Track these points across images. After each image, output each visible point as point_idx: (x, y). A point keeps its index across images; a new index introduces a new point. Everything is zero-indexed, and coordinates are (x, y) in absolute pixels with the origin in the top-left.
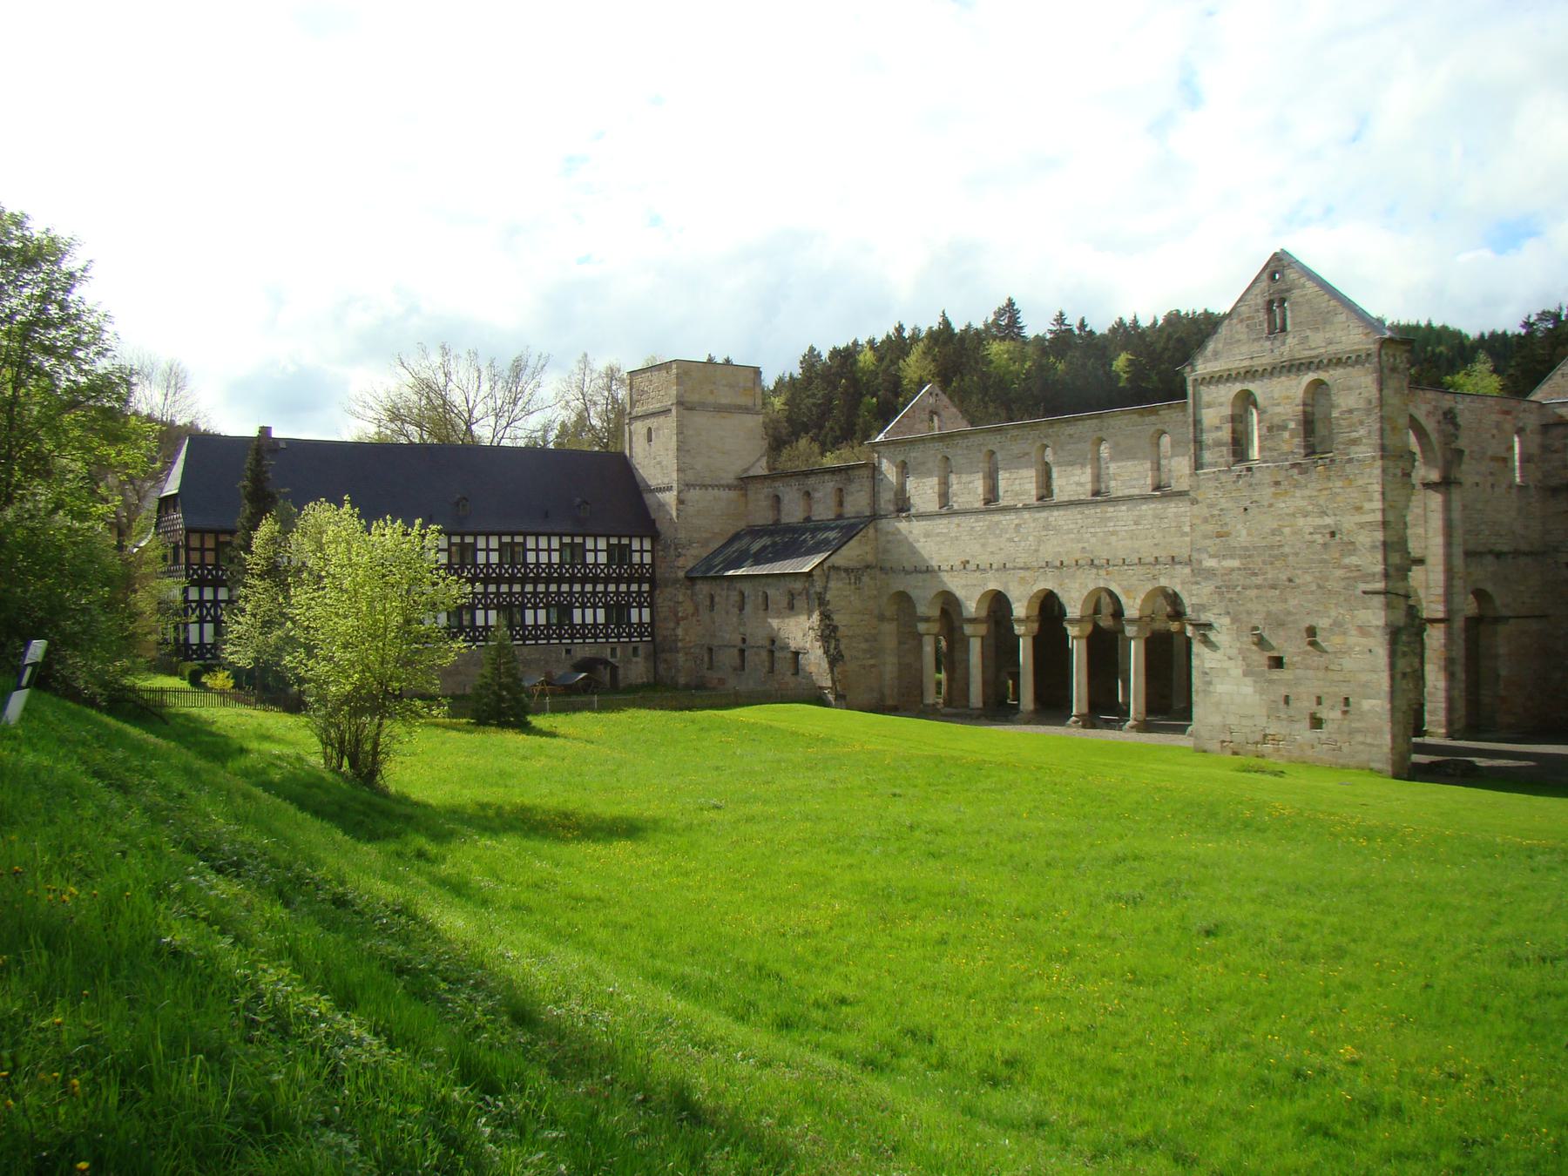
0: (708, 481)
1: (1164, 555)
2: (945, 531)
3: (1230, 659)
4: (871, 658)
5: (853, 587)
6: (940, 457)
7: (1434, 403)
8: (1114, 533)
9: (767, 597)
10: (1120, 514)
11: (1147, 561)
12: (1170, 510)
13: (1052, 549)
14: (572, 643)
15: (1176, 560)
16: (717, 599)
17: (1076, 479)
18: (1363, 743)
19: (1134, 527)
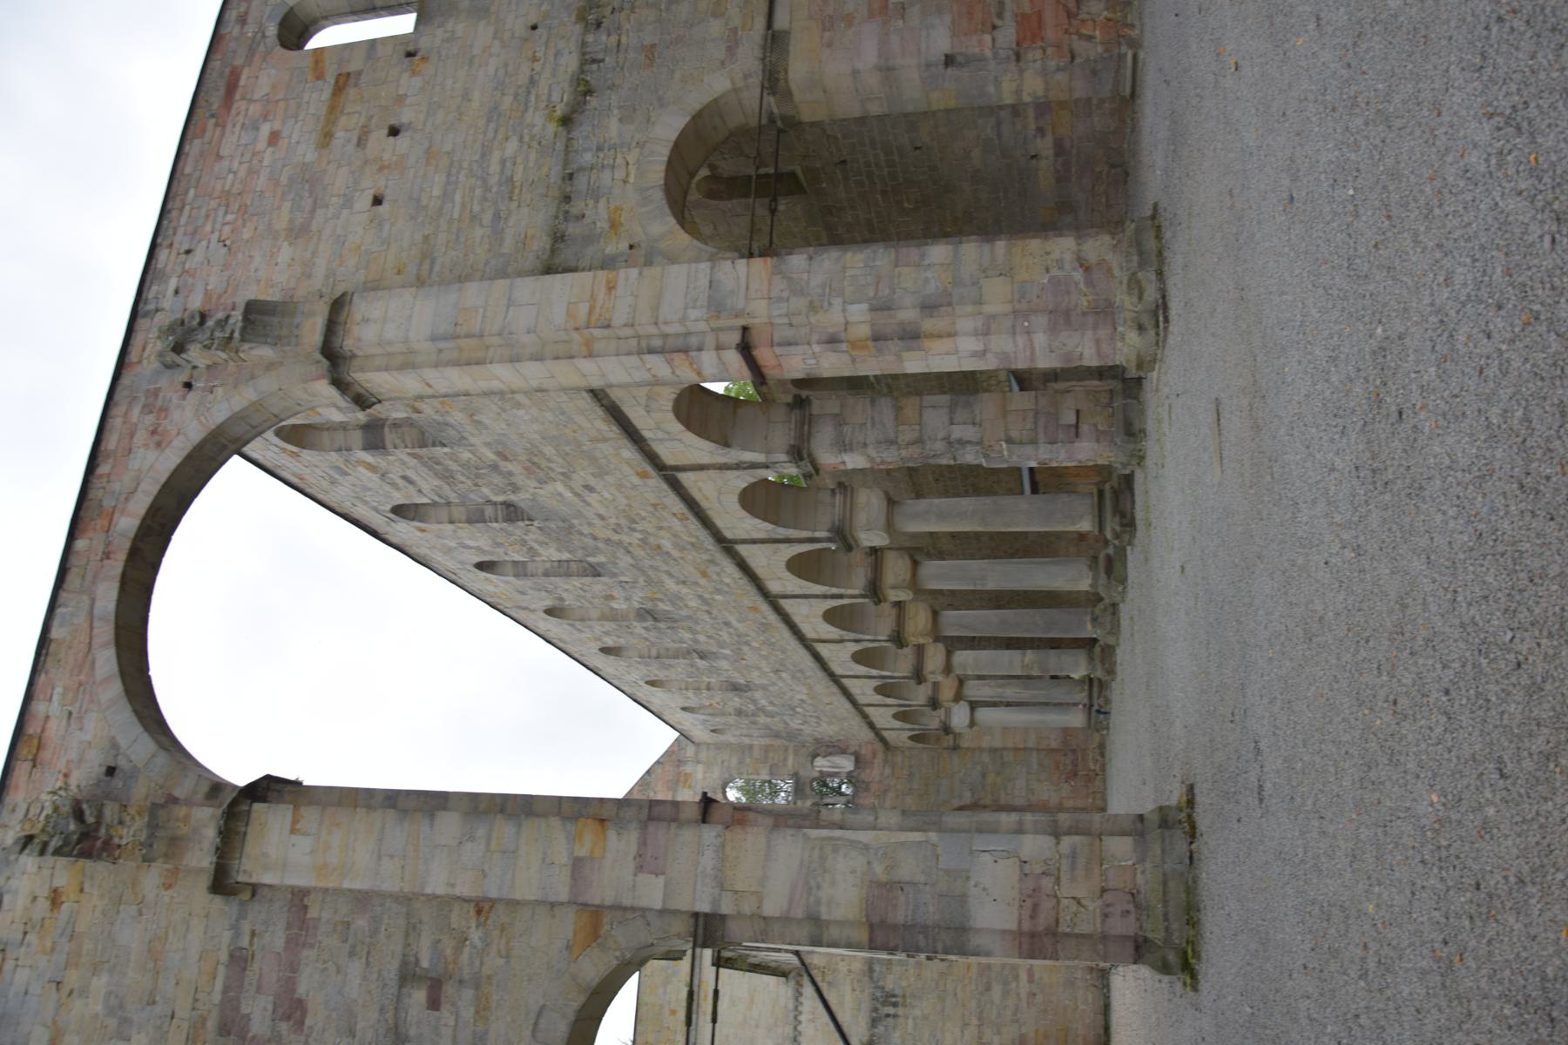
0: (789, 1030)
4: (1017, 978)
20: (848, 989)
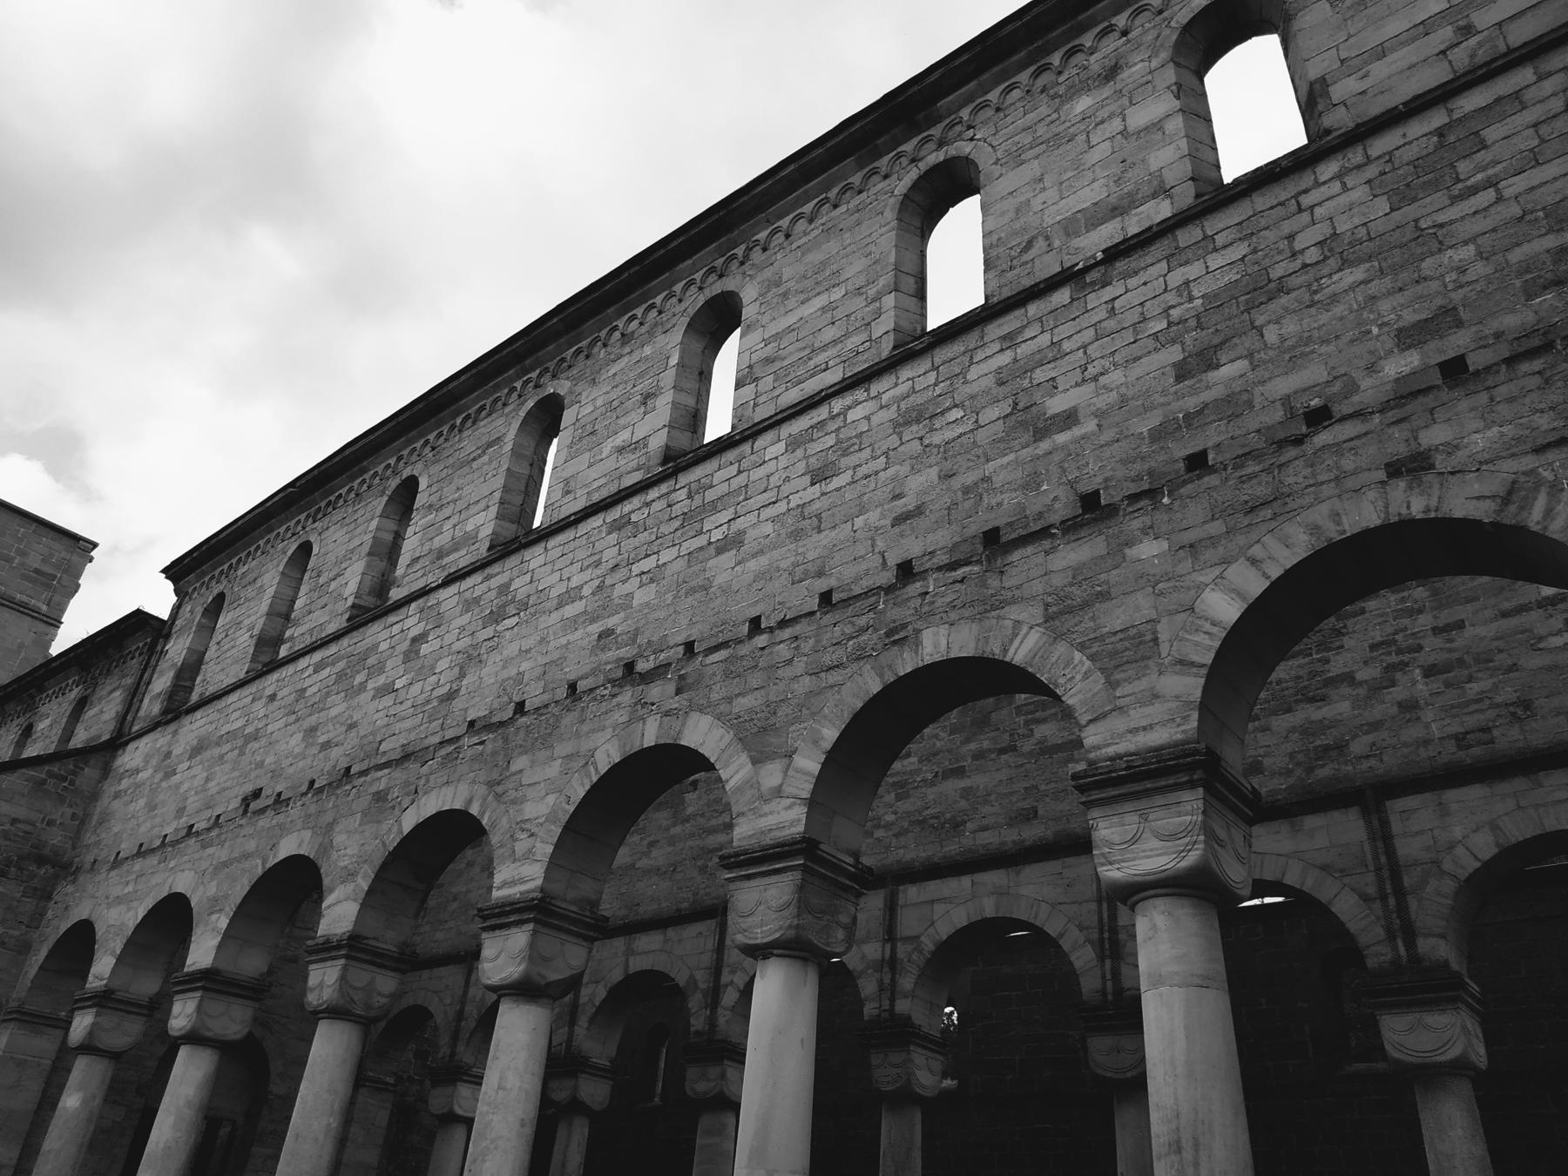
10: (757, 474)
12: (973, 374)
17: (623, 437)
20: (21, 812)
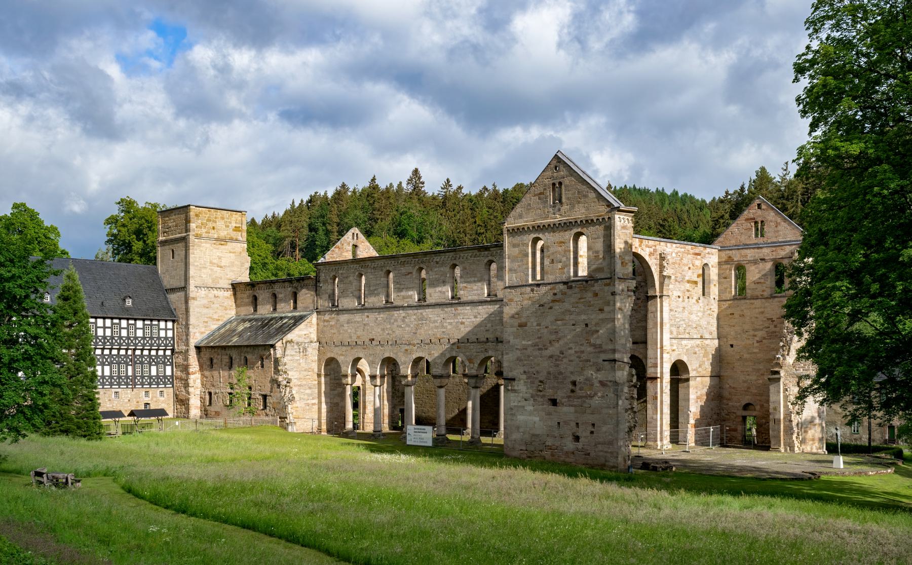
1: (491, 336)
2: (360, 320)
3: (526, 400)
5: (302, 354)
6: (357, 273)
7: (654, 247)
8: (462, 323)
9: (246, 360)
10: (466, 311)
11: (482, 340)
13: (425, 333)
14: (119, 388)
15: (499, 340)
16: (215, 361)
18: (602, 451)
19: (474, 320)
20: (305, 333)
